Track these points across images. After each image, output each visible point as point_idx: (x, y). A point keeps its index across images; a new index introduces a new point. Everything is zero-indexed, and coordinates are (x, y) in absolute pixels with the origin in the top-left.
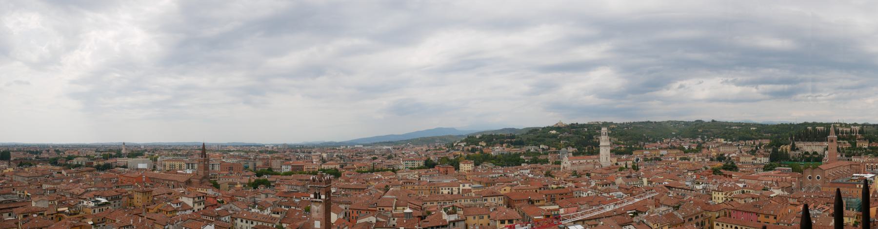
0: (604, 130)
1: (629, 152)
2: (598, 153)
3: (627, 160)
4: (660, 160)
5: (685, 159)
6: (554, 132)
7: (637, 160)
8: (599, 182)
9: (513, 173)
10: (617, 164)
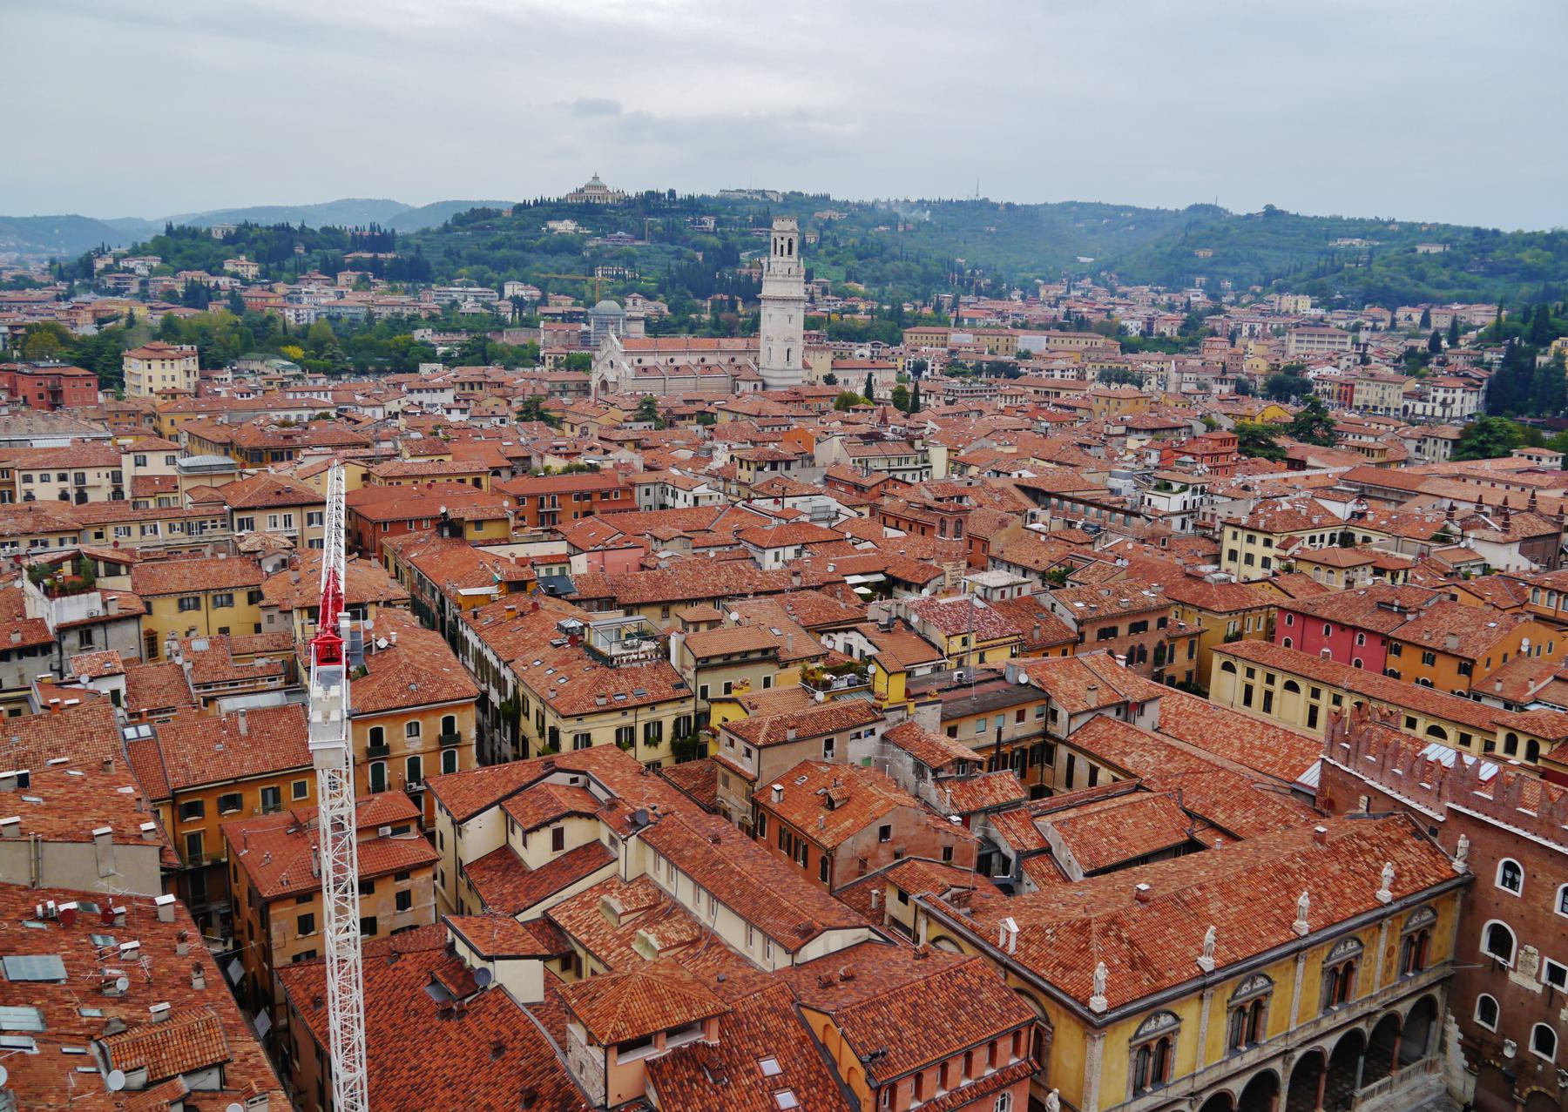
0: (784, 227)
1: (889, 328)
2: (753, 327)
3: (874, 364)
4: (1012, 373)
5: (1123, 377)
6: (566, 227)
7: (919, 368)
8: (748, 451)
9: (377, 402)
10: (830, 380)
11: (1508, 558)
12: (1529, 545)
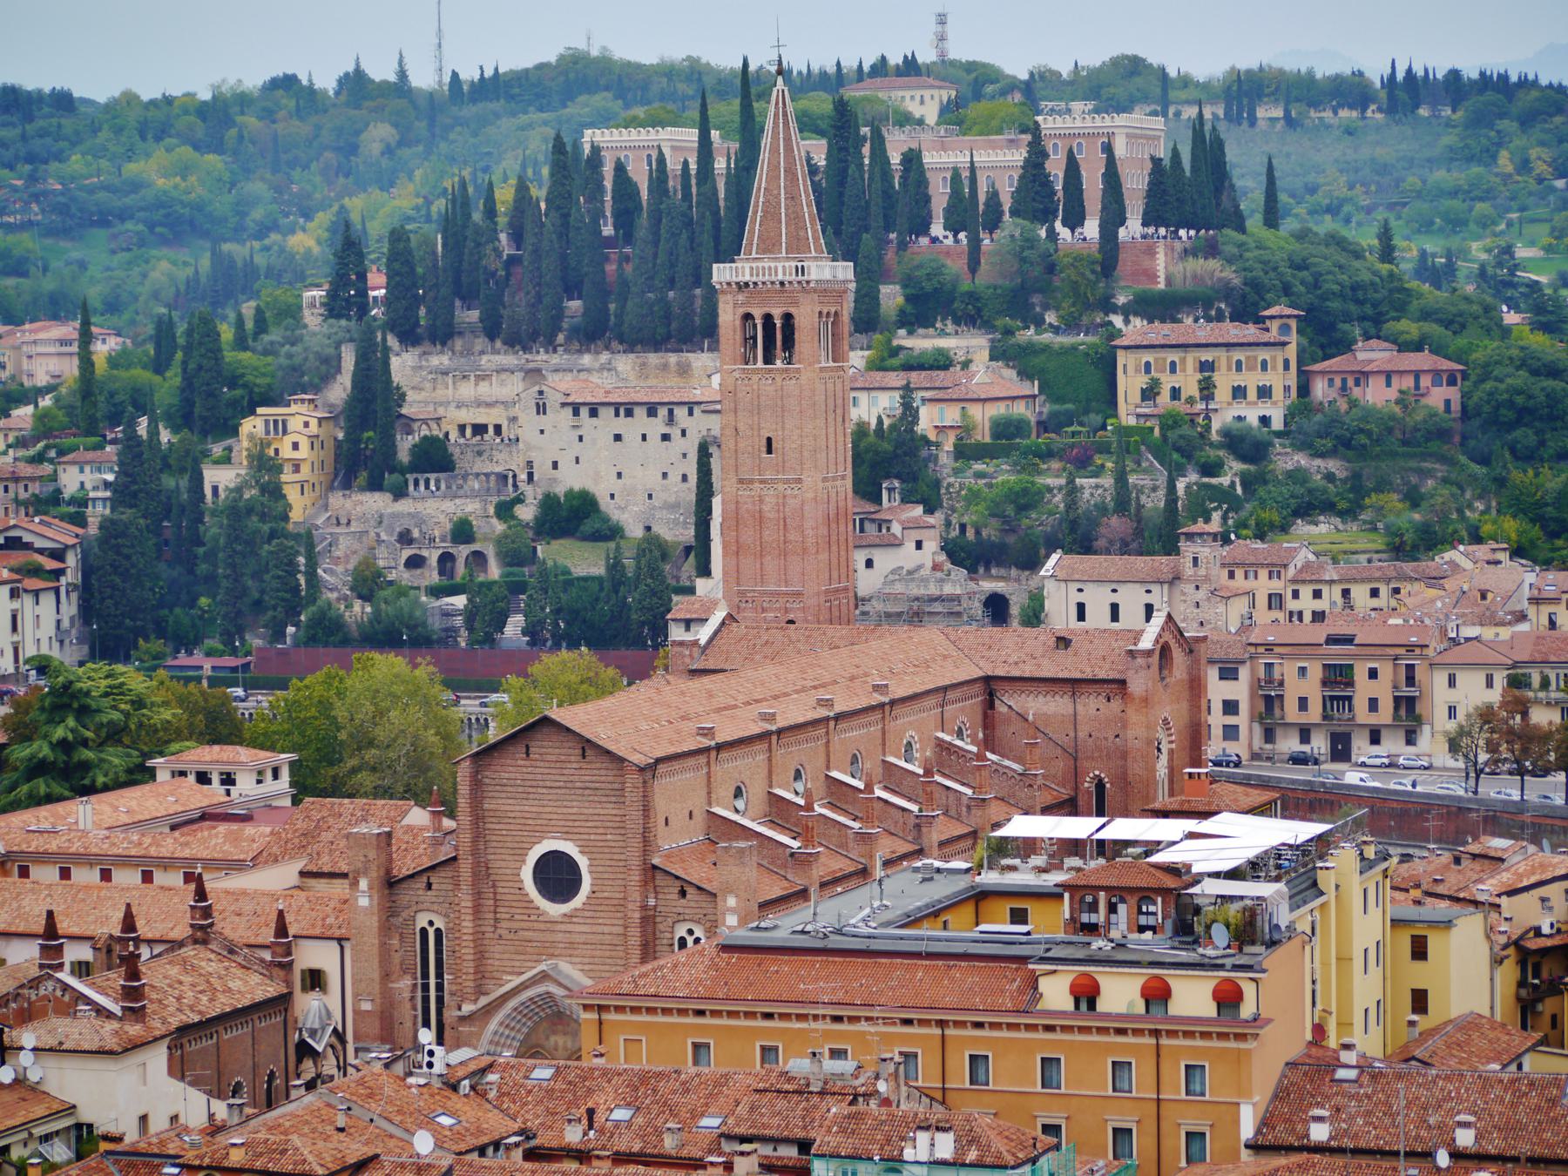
11: (137, 1096)
12: (194, 1047)
